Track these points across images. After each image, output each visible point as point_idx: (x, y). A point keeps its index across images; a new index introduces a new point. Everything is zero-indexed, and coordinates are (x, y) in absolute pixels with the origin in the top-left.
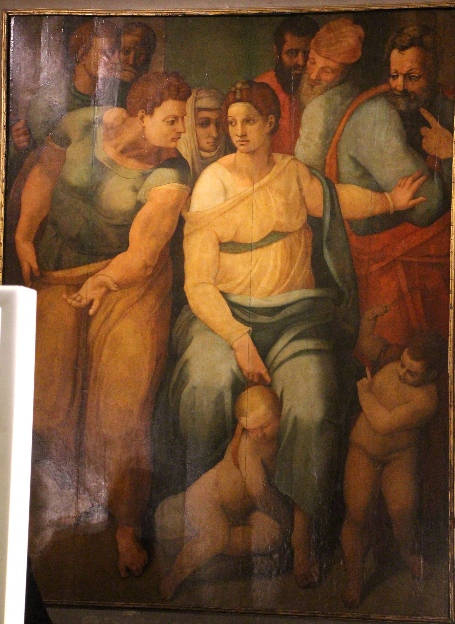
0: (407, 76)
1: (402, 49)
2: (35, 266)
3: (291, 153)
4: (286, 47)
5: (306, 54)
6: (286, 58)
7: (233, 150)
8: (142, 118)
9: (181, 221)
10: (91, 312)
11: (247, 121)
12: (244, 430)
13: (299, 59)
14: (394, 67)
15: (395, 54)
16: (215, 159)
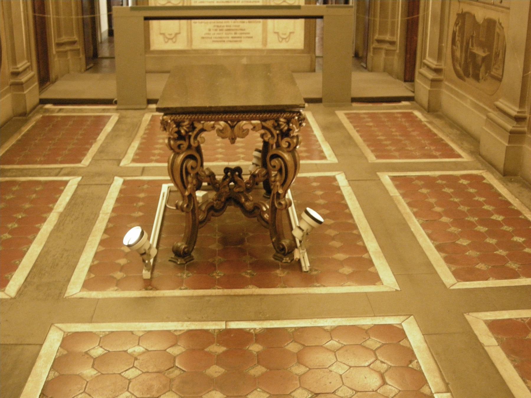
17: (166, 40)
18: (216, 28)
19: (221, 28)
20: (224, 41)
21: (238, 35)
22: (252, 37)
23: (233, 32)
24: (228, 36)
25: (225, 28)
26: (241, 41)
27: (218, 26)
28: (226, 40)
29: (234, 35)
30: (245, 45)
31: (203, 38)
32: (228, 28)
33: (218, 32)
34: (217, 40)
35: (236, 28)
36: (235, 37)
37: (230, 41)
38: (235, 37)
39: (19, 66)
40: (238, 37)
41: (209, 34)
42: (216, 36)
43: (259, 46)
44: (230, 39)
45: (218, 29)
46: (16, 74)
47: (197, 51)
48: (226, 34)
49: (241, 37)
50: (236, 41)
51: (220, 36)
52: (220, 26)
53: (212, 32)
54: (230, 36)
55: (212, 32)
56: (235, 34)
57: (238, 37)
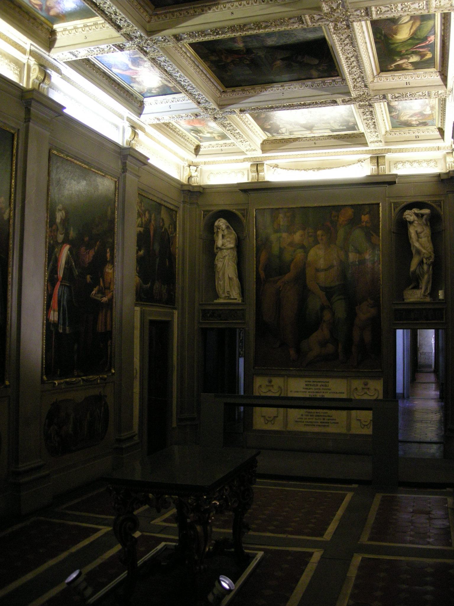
0: (366, 222)
1: (365, 215)
2: (264, 277)
3: (335, 244)
4: (333, 215)
5: (338, 216)
6: (333, 218)
7: (319, 243)
8: (293, 235)
9: (305, 264)
10: (280, 289)
11: (322, 235)
12: (324, 321)
13: (336, 218)
14: (362, 220)
15: (363, 216)
16: (313, 247)
17: (266, 422)
18: (307, 414)
20: (314, 425)
21: (325, 421)
22: (338, 423)
24: (318, 421)
25: (315, 414)
26: (328, 426)
27: (309, 412)
29: (322, 421)
30: (332, 429)
31: (297, 421)
32: (317, 414)
33: (309, 417)
34: (309, 424)
36: (324, 423)
38: (324, 423)
39: (122, 435)
41: (301, 418)
42: (307, 420)
43: (344, 431)
44: (320, 424)
46: (119, 441)
47: (289, 432)
50: (324, 426)
51: (310, 420)
52: (311, 412)
53: (304, 417)
55: (304, 417)
56: (324, 419)
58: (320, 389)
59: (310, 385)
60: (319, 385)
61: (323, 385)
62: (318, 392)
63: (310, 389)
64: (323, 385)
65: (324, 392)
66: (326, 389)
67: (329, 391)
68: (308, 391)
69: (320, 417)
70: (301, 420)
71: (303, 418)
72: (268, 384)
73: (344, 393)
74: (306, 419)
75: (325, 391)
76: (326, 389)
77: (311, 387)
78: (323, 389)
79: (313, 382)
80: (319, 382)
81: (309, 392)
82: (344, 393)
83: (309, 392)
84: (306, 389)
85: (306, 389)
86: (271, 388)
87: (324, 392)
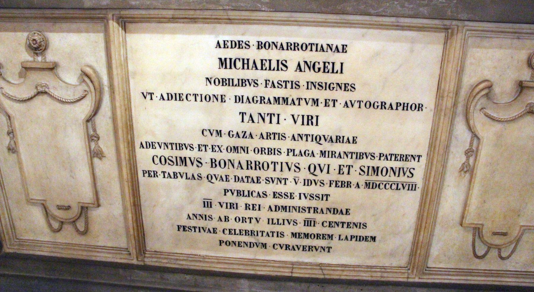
18: (230, 198)
19: (250, 201)
21: (317, 230)
22: (374, 239)
23: (300, 217)
25: (271, 201)
27: (240, 193)
28: (270, 241)
29: (301, 228)
35: (314, 203)
36: (307, 236)
37: (287, 247)
38: (307, 236)
40: (318, 236)
41: (204, 217)
42: (232, 224)
44: (288, 240)
45: (242, 201)
48: (270, 221)
49: (331, 237)
52: (250, 194)
54: (288, 229)
55: (216, 212)
56: (308, 223)
57: (318, 236)
58: (296, 85)
59: (245, 63)
60: (292, 66)
61: (312, 66)
62: (285, 100)
63: (243, 83)
64: (312, 66)
65: (316, 102)
66: (329, 87)
67: (342, 96)
68: (231, 92)
69: (294, 215)
70: (201, 223)
71: (211, 218)
72: (26, 57)
73: (419, 107)
74: (227, 219)
75: (322, 95)
76: (329, 87)
77: (250, 74)
78: (311, 85)
79: (260, 46)
80: (294, 47)
81: (239, 99)
82: (419, 107)
83: (239, 99)
84: (224, 82)
85: (224, 82)
86: (45, 79)
87: (316, 102)
